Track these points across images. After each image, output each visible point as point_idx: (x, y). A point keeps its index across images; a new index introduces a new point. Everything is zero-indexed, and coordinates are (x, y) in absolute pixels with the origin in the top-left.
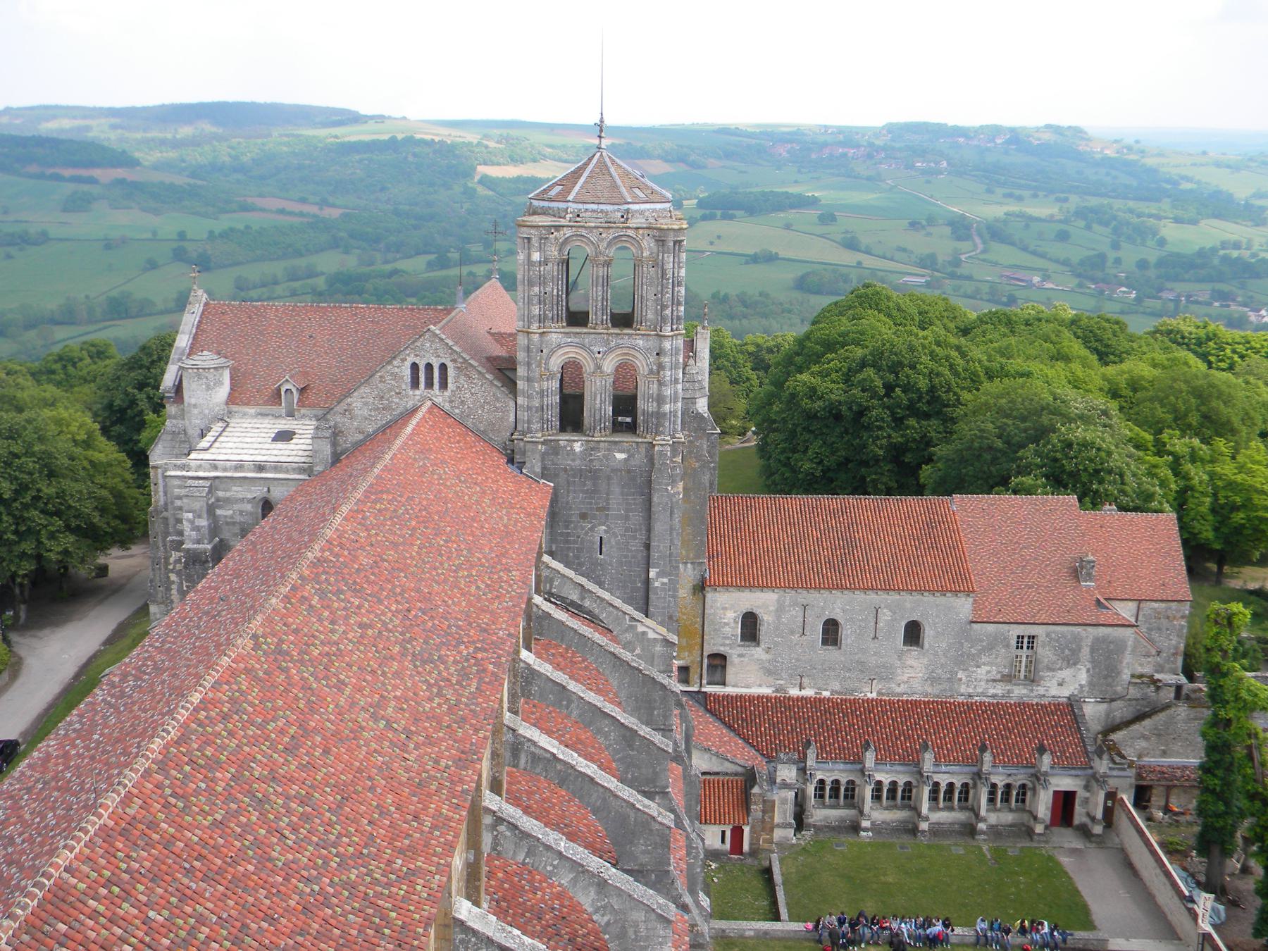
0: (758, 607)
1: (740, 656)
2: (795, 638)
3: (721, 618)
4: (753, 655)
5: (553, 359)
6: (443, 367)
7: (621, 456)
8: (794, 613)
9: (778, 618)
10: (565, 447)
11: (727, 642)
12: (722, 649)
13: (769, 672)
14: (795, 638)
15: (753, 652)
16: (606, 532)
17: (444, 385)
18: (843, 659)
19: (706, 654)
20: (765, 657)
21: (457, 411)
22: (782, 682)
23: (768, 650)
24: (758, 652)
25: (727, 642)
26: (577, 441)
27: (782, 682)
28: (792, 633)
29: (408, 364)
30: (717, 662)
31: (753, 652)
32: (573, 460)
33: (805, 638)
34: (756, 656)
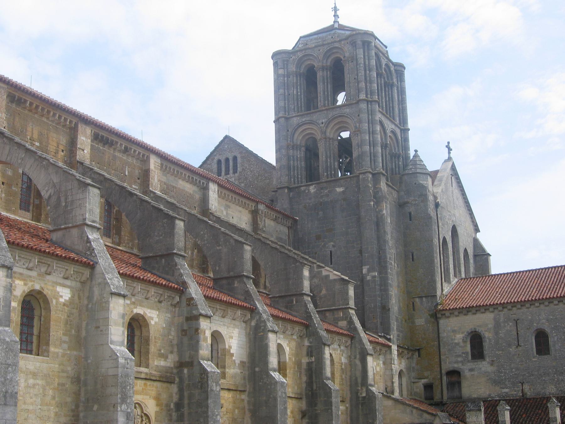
0: (478, 326)
1: (471, 370)
2: (512, 349)
3: (452, 339)
4: (480, 369)
5: (296, 136)
6: (235, 158)
7: (339, 190)
8: (508, 328)
9: (497, 333)
10: (305, 191)
11: (460, 359)
12: (456, 365)
13: (496, 382)
14: (512, 349)
15: (481, 366)
16: (334, 246)
17: (235, 171)
18: (554, 364)
19: (444, 372)
20: (490, 369)
21: (243, 185)
22: (506, 390)
23: (492, 363)
24: (484, 366)
25: (460, 359)
26: (312, 185)
27: (506, 390)
28: (510, 345)
29: (215, 161)
30: (454, 379)
31: (481, 366)
32: (310, 199)
33: (520, 348)
34: (483, 369)
